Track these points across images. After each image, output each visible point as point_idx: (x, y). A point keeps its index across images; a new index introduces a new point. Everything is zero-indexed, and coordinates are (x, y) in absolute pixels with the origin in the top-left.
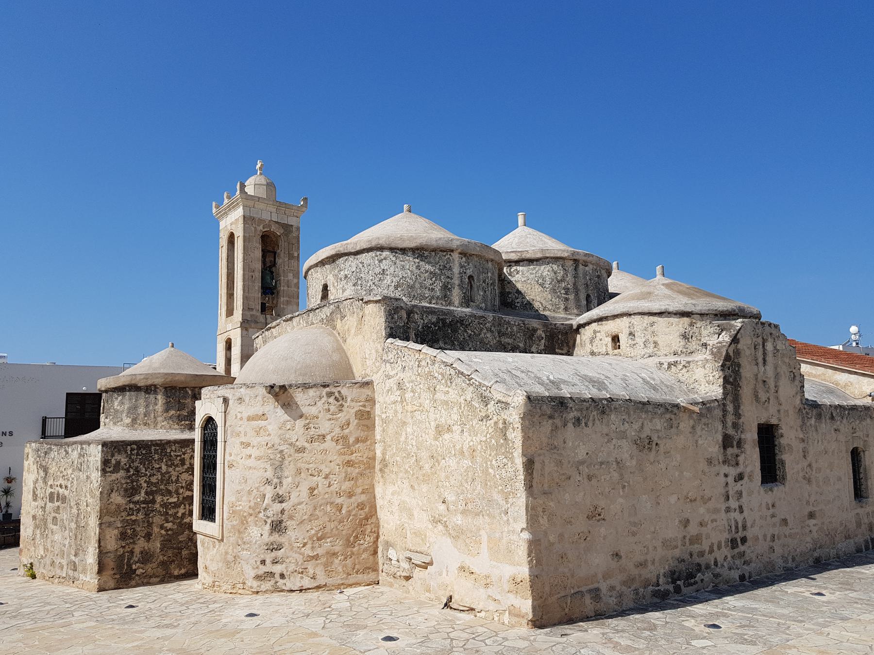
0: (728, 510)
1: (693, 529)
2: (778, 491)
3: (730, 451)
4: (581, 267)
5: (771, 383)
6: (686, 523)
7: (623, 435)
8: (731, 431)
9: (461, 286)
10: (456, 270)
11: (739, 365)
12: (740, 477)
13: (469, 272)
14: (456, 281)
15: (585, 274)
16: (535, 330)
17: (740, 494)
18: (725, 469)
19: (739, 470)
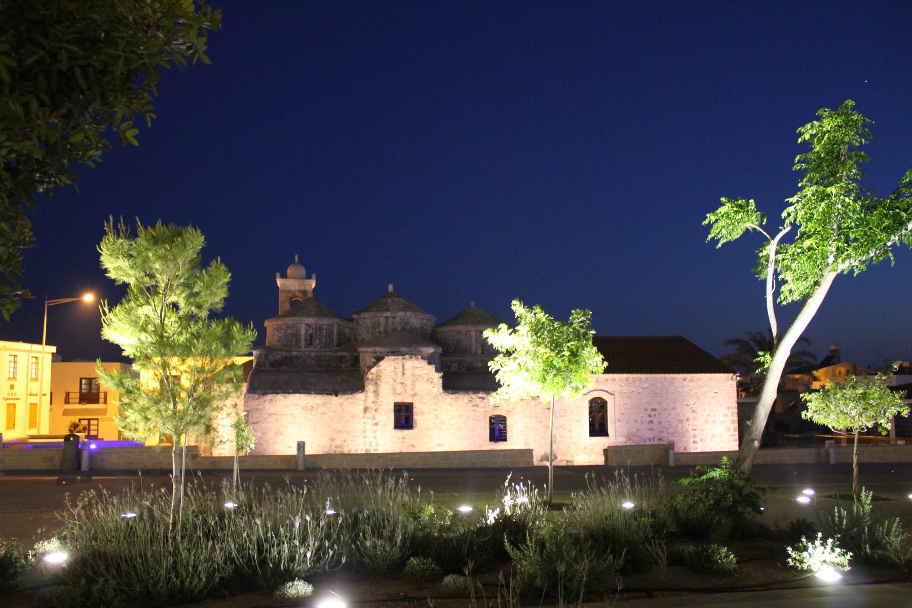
0: (365, 437)
1: (338, 442)
2: (406, 432)
3: (368, 415)
4: (390, 320)
5: (409, 383)
6: (333, 440)
7: (296, 405)
8: (370, 404)
9: (306, 340)
10: (303, 331)
11: (380, 376)
12: (376, 424)
13: (310, 332)
14: (303, 337)
15: (393, 323)
16: (344, 357)
17: (375, 431)
18: (365, 420)
19: (375, 421)
